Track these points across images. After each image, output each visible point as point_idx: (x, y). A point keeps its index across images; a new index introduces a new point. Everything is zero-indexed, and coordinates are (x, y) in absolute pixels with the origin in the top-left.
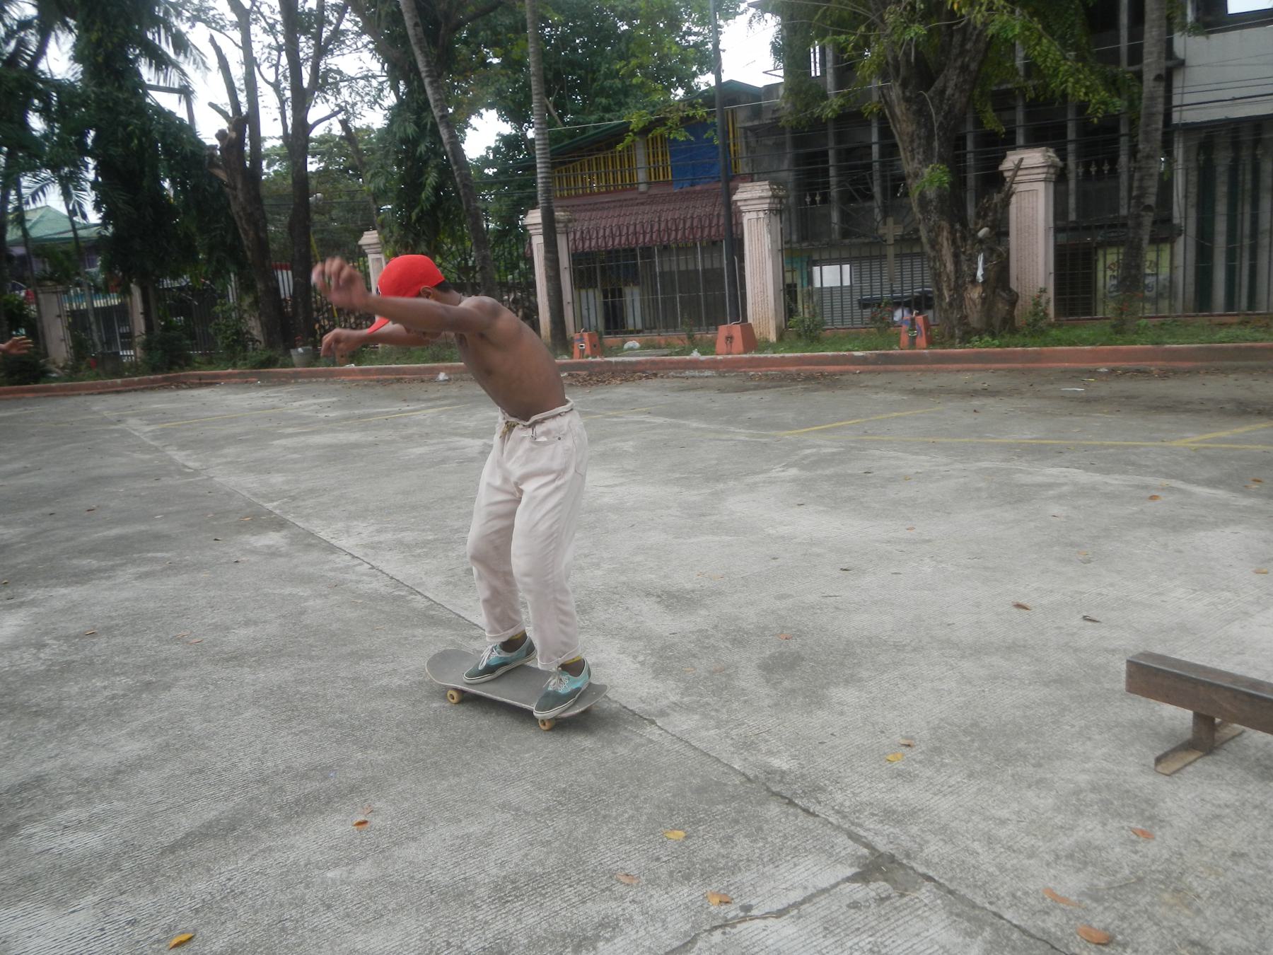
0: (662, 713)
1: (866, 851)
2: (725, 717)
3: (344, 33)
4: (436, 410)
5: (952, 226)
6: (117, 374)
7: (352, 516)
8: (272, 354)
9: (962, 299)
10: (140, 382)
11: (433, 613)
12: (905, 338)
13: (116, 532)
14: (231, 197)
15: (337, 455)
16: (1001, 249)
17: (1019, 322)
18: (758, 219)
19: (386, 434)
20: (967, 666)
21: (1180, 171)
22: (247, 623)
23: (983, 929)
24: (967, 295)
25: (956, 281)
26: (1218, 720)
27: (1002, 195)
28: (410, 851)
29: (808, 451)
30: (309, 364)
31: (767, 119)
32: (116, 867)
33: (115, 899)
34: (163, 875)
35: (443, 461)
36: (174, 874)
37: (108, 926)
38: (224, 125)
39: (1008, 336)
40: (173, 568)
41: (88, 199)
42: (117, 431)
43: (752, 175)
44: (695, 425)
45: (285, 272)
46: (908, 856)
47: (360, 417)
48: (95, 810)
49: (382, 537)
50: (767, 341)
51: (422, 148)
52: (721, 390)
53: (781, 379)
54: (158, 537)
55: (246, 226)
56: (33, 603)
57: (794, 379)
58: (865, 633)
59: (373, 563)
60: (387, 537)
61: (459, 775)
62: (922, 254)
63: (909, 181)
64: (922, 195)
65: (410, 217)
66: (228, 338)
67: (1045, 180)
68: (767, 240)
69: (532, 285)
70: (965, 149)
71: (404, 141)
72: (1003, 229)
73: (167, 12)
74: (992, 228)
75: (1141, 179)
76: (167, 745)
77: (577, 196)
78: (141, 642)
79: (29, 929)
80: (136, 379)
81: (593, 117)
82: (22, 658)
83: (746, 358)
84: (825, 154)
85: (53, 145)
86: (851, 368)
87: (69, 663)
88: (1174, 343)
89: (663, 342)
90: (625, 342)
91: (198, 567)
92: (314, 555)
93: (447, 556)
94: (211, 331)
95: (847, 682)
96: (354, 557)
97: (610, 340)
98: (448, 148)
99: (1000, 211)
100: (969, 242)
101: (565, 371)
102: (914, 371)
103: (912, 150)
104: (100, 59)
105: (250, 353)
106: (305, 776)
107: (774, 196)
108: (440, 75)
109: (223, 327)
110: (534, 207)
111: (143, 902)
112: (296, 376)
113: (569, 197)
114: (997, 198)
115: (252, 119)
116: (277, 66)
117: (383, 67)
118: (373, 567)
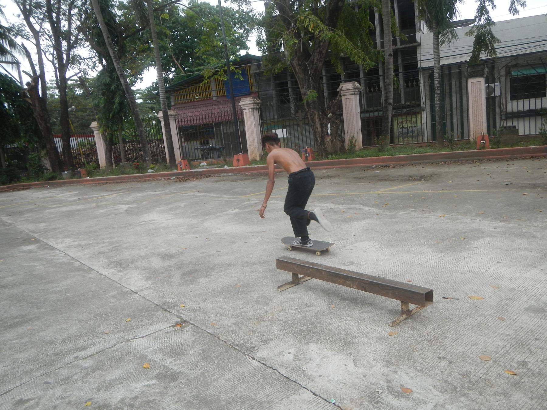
0: (142, 290)
1: (179, 320)
2: (160, 290)
3: (81, 39)
4: (116, 195)
5: (319, 113)
8: (54, 174)
18: (249, 112)
19: (94, 205)
21: (422, 87)
22: (12, 276)
23: (198, 334)
24: (325, 139)
26: (300, 276)
28: (42, 334)
29: (247, 203)
31: (263, 68)
35: (110, 215)
38: (29, 80)
39: (341, 155)
43: (259, 92)
44: (212, 195)
46: (190, 320)
47: (86, 199)
51: (113, 87)
52: (232, 181)
58: (222, 262)
59: (66, 253)
60: (77, 243)
63: (303, 96)
64: (307, 102)
66: (35, 169)
67: (354, 94)
68: (253, 120)
70: (341, 79)
71: (105, 85)
72: (341, 113)
77: (188, 103)
81: (195, 69)
83: (244, 168)
84: (287, 83)
89: (216, 162)
90: (201, 163)
92: (46, 251)
94: (28, 166)
95: (206, 276)
96: (60, 251)
97: (195, 162)
98: (124, 87)
100: (325, 119)
101: (173, 176)
103: (303, 84)
105: (46, 174)
106: (16, 318)
107: (255, 103)
108: (120, 58)
109: (33, 164)
112: (64, 183)
113: (185, 103)
117: (96, 55)
118: (66, 254)
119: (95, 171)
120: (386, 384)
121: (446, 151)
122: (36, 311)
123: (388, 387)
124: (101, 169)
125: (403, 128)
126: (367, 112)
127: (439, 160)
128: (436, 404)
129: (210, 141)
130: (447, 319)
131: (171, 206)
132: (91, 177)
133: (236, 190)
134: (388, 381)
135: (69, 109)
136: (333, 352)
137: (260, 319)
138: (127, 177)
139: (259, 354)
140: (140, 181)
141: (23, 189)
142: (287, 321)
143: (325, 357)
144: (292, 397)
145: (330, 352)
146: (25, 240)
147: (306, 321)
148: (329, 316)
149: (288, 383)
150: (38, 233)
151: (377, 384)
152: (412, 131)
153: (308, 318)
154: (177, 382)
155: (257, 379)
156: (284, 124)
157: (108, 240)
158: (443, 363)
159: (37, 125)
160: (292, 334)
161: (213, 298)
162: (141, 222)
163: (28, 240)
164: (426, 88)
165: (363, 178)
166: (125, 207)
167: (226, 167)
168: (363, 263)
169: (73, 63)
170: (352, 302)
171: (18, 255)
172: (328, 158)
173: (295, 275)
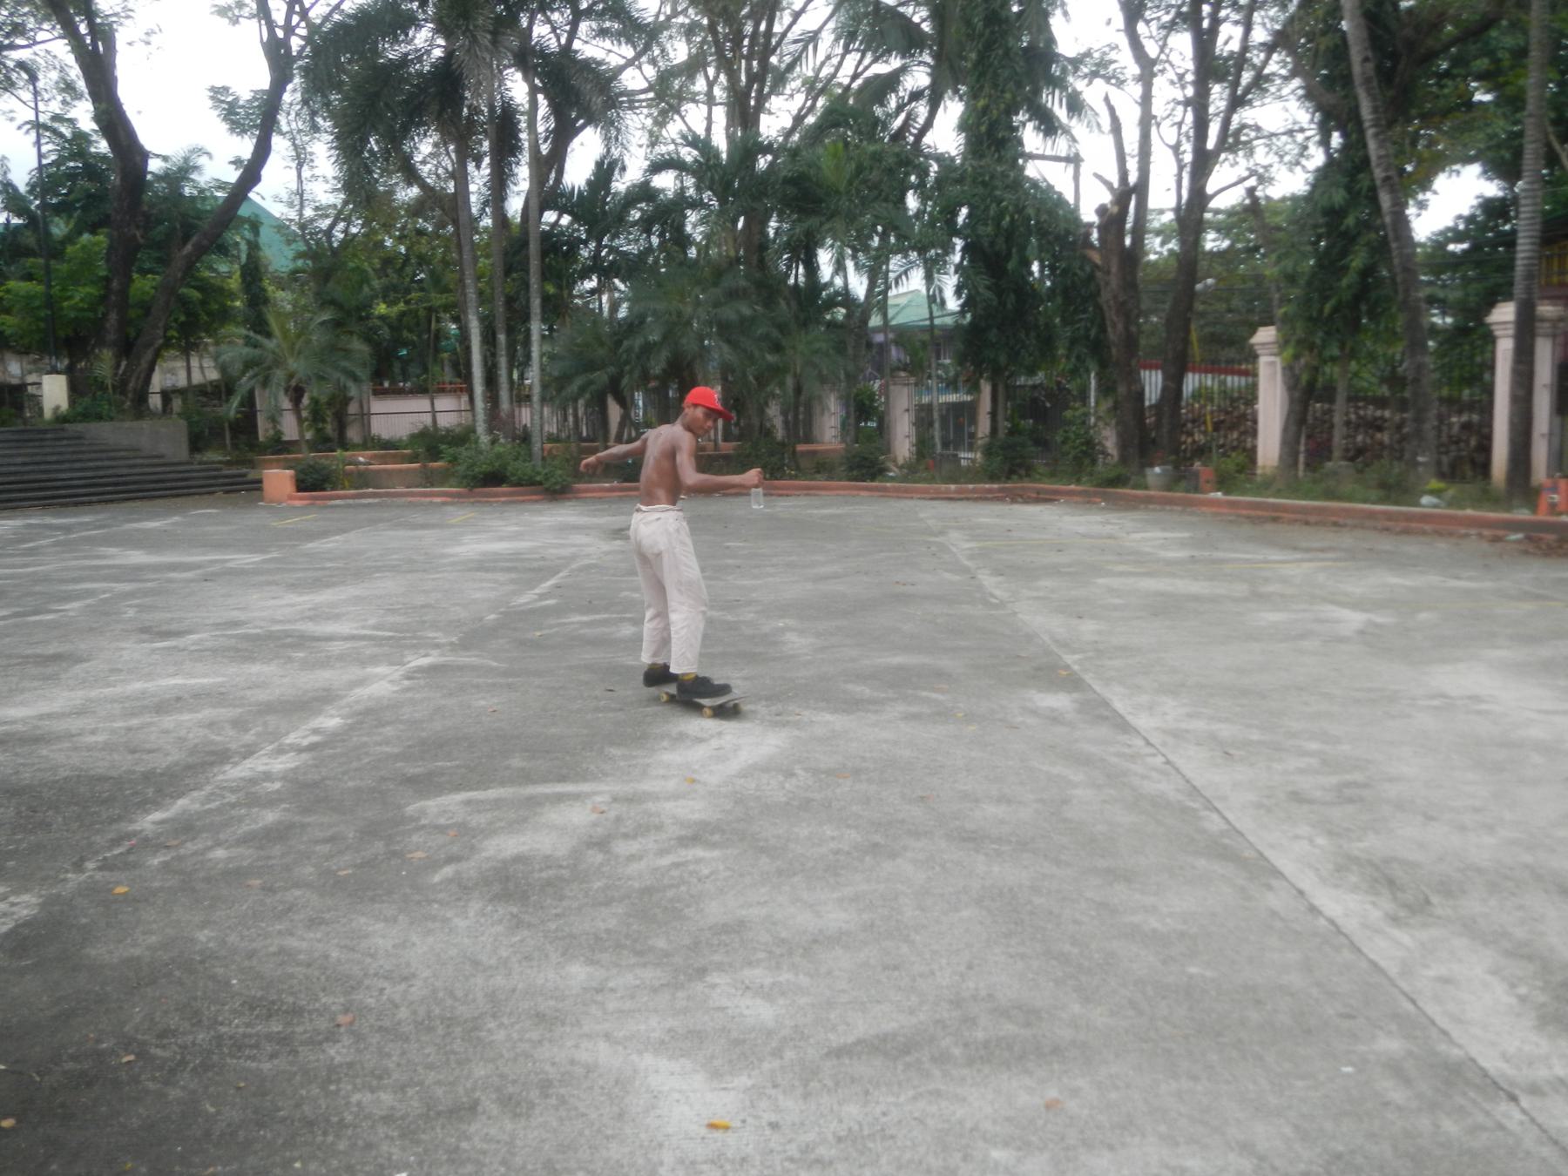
0: (1535, 1090)
3: (1269, 78)
4: (1312, 565)
6: (953, 479)
10: (974, 491)
11: (1226, 841)
13: (899, 660)
14: (1102, 283)
19: (1241, 589)
22: (1002, 799)
32: (777, 1053)
33: (767, 1091)
34: (820, 1081)
35: (1303, 636)
36: (830, 1083)
37: (750, 1120)
38: (1106, 198)
40: (942, 715)
41: (949, 282)
47: (1214, 562)
48: (781, 979)
51: (1350, 221)
54: (940, 674)
55: (1115, 318)
59: (1172, 757)
60: (1200, 725)
65: (1321, 311)
66: (1075, 448)
69: (1487, 409)
73: (1064, 70)
76: (872, 925)
79: (680, 1092)
80: (971, 486)
82: (768, 784)
85: (923, 225)
87: (809, 801)
91: (969, 718)
92: (1103, 731)
96: (1148, 743)
98: (1388, 219)
104: (983, 129)
105: (1100, 467)
108: (1391, 124)
109: (1072, 436)
110: (1508, 297)
111: (791, 1106)
112: (1148, 501)
115: (1142, 189)
116: (1180, 124)
117: (1312, 121)
118: (1168, 762)
119: (1242, 476)
122: (1076, 1008)
124: (1259, 471)
131: (1545, 652)
132: (1226, 493)
135: (1199, 287)
140: (1387, 529)
146: (1038, 669)
150: (1074, 652)
157: (1314, 746)
159: (1102, 329)
162: (1433, 697)
163: (1052, 675)
166: (1353, 619)
169: (1233, 149)
171: (1020, 719)
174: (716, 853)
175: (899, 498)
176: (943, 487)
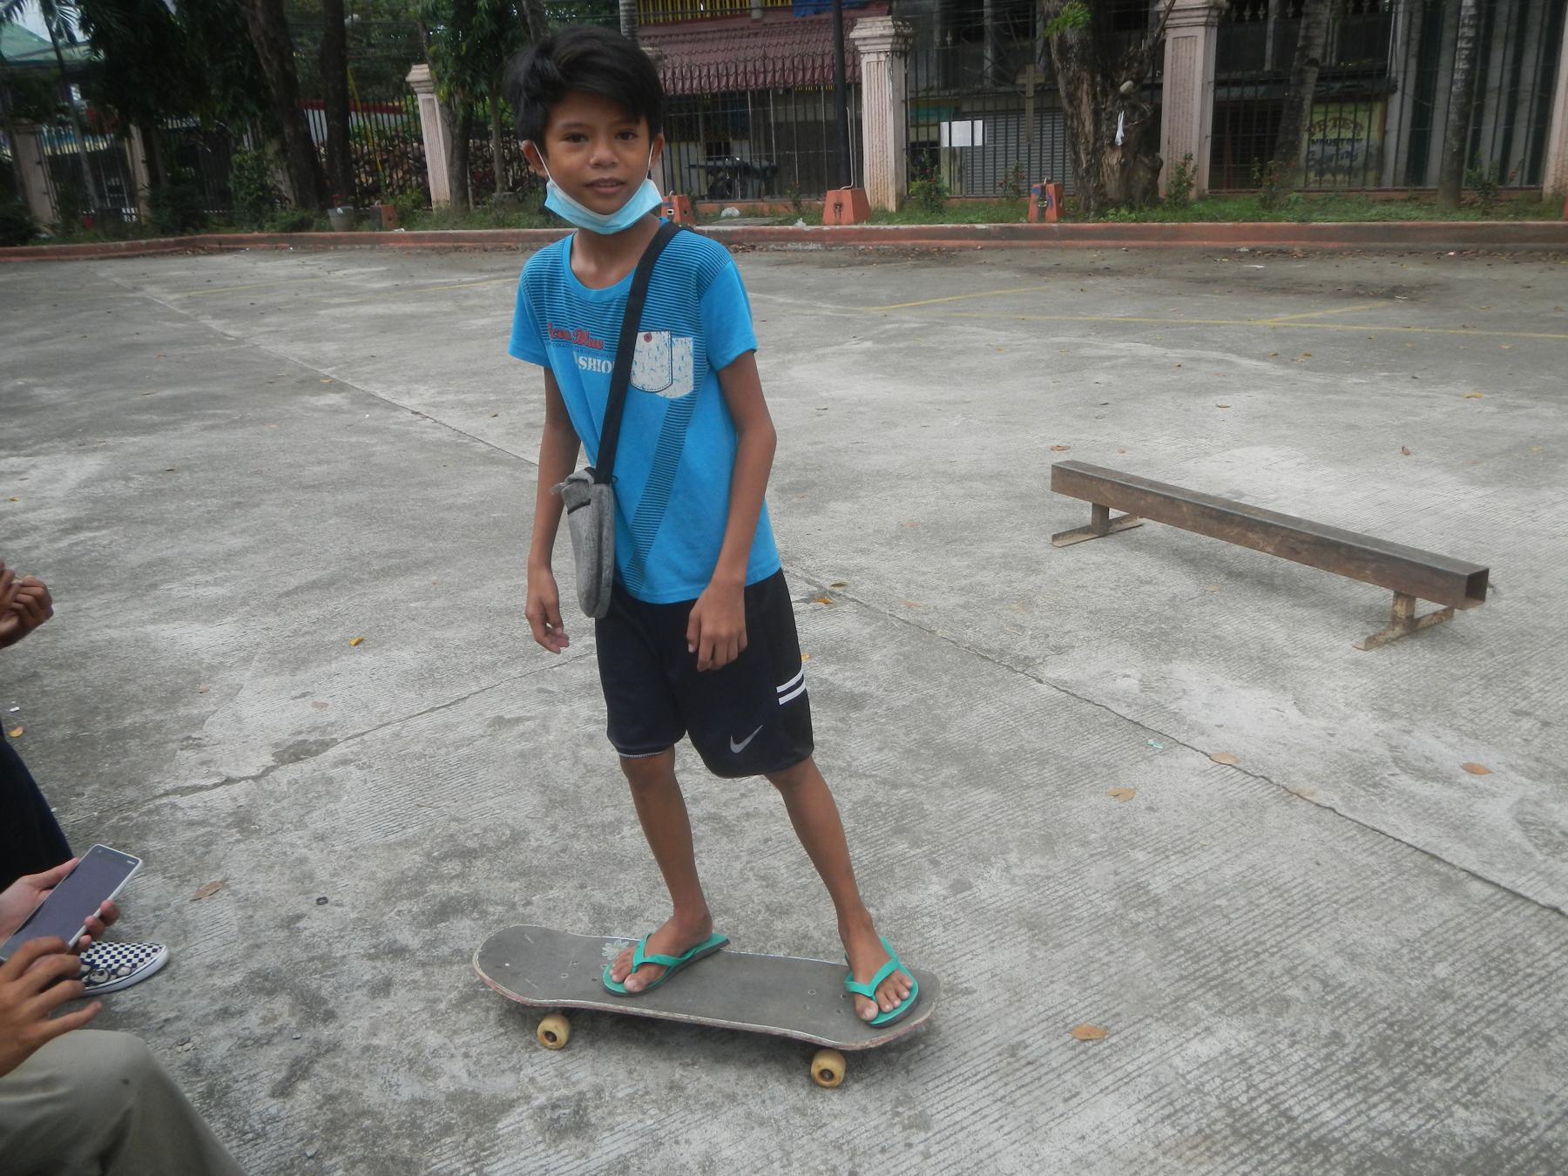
5: (1093, 78)
7: (411, 381)
8: (306, 214)
9: (1100, 165)
10: (148, 246)
12: (1034, 209)
13: (167, 393)
14: (249, 18)
15: (388, 325)
16: (1145, 107)
17: (1162, 192)
18: (878, 62)
19: (447, 306)
20: (950, 489)
22: (320, 463)
25: (1094, 144)
26: (1114, 513)
27: (1150, 42)
28: (475, 593)
29: (890, 326)
30: (350, 228)
32: (244, 603)
39: (1146, 209)
42: (138, 299)
44: (781, 300)
45: (316, 112)
49: (445, 398)
50: (885, 211)
52: (824, 265)
53: (894, 254)
54: (214, 397)
56: (106, 448)
57: (905, 254)
60: (451, 397)
61: (513, 554)
62: (1060, 109)
64: (1062, 39)
67: (1206, 24)
74: (1136, 81)
75: (1308, 27)
76: (267, 540)
77: (675, 23)
78: (223, 476)
80: (143, 242)
86: (973, 243)
87: (160, 491)
88: (1323, 220)
89: (766, 209)
90: (722, 209)
92: (378, 412)
93: (508, 414)
94: (231, 185)
95: (846, 499)
97: (706, 206)
99: (1147, 61)
100: (1110, 97)
102: (1040, 247)
105: (280, 213)
107: (897, 35)
109: (245, 181)
111: (272, 620)
112: (336, 241)
113: (666, 23)
114: (1144, 46)
120: (1388, 754)
121: (1465, 219)
123: (1396, 760)
124: (434, 206)
125: (1324, 142)
126: (1236, 83)
127: (1442, 245)
128: (1521, 801)
129: (734, 145)
130: (1523, 635)
133: (847, 291)
134: (1393, 748)
135: (347, 21)
136: (1238, 683)
137: (1026, 602)
138: (513, 235)
139: (1050, 673)
141: (221, 251)
142: (1098, 611)
143: (1220, 690)
144: (1160, 760)
145: (1230, 682)
146: (302, 381)
147: (1147, 614)
148: (1207, 609)
149: (1142, 732)
151: (1365, 751)
152: (1351, 155)
153: (1153, 609)
154: (865, 712)
155: (1061, 721)
156: (957, 109)
158: (1526, 724)
160: (1122, 638)
161: (883, 549)
163: (311, 383)
164: (1414, 20)
165: (1215, 281)
167: (800, 225)
168: (1272, 497)
170: (1260, 583)
172: (1104, 216)
173: (1101, 510)
174: (104, 532)
175: (63, 261)
176: (111, 244)
